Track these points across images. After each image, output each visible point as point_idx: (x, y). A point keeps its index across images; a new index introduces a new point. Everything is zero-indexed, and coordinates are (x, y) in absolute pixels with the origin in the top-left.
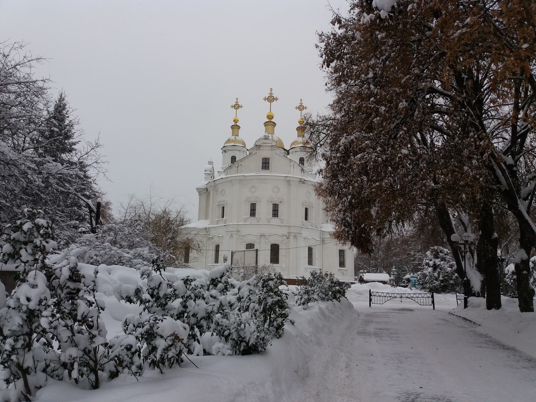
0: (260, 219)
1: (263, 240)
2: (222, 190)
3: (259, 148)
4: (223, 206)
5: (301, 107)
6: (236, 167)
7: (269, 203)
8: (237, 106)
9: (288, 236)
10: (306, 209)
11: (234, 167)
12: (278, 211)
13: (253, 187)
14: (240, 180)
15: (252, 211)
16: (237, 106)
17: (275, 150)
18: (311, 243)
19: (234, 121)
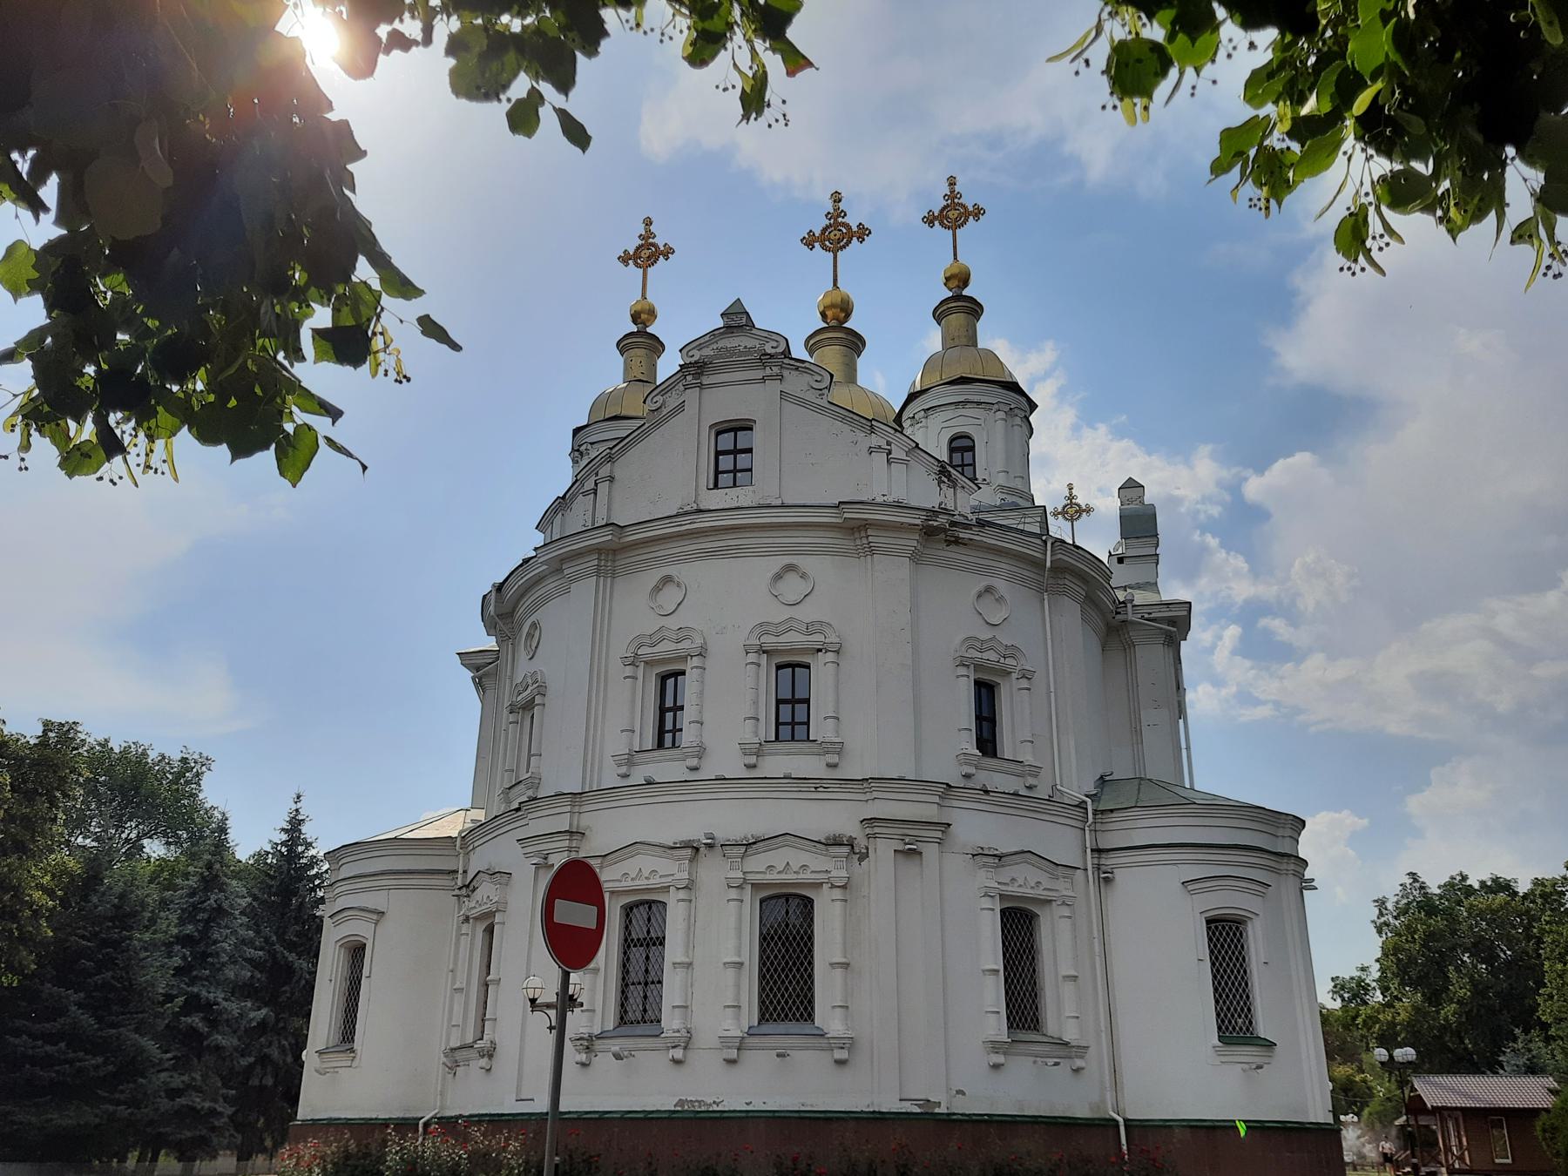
0: (701, 751)
1: (714, 873)
2: (534, 626)
3: (698, 375)
5: (953, 214)
6: (585, 494)
7: (752, 657)
8: (647, 254)
9: (861, 842)
10: (985, 692)
12: (807, 701)
13: (667, 580)
14: (598, 550)
16: (645, 253)
17: (781, 378)
18: (1025, 881)
19: (635, 318)
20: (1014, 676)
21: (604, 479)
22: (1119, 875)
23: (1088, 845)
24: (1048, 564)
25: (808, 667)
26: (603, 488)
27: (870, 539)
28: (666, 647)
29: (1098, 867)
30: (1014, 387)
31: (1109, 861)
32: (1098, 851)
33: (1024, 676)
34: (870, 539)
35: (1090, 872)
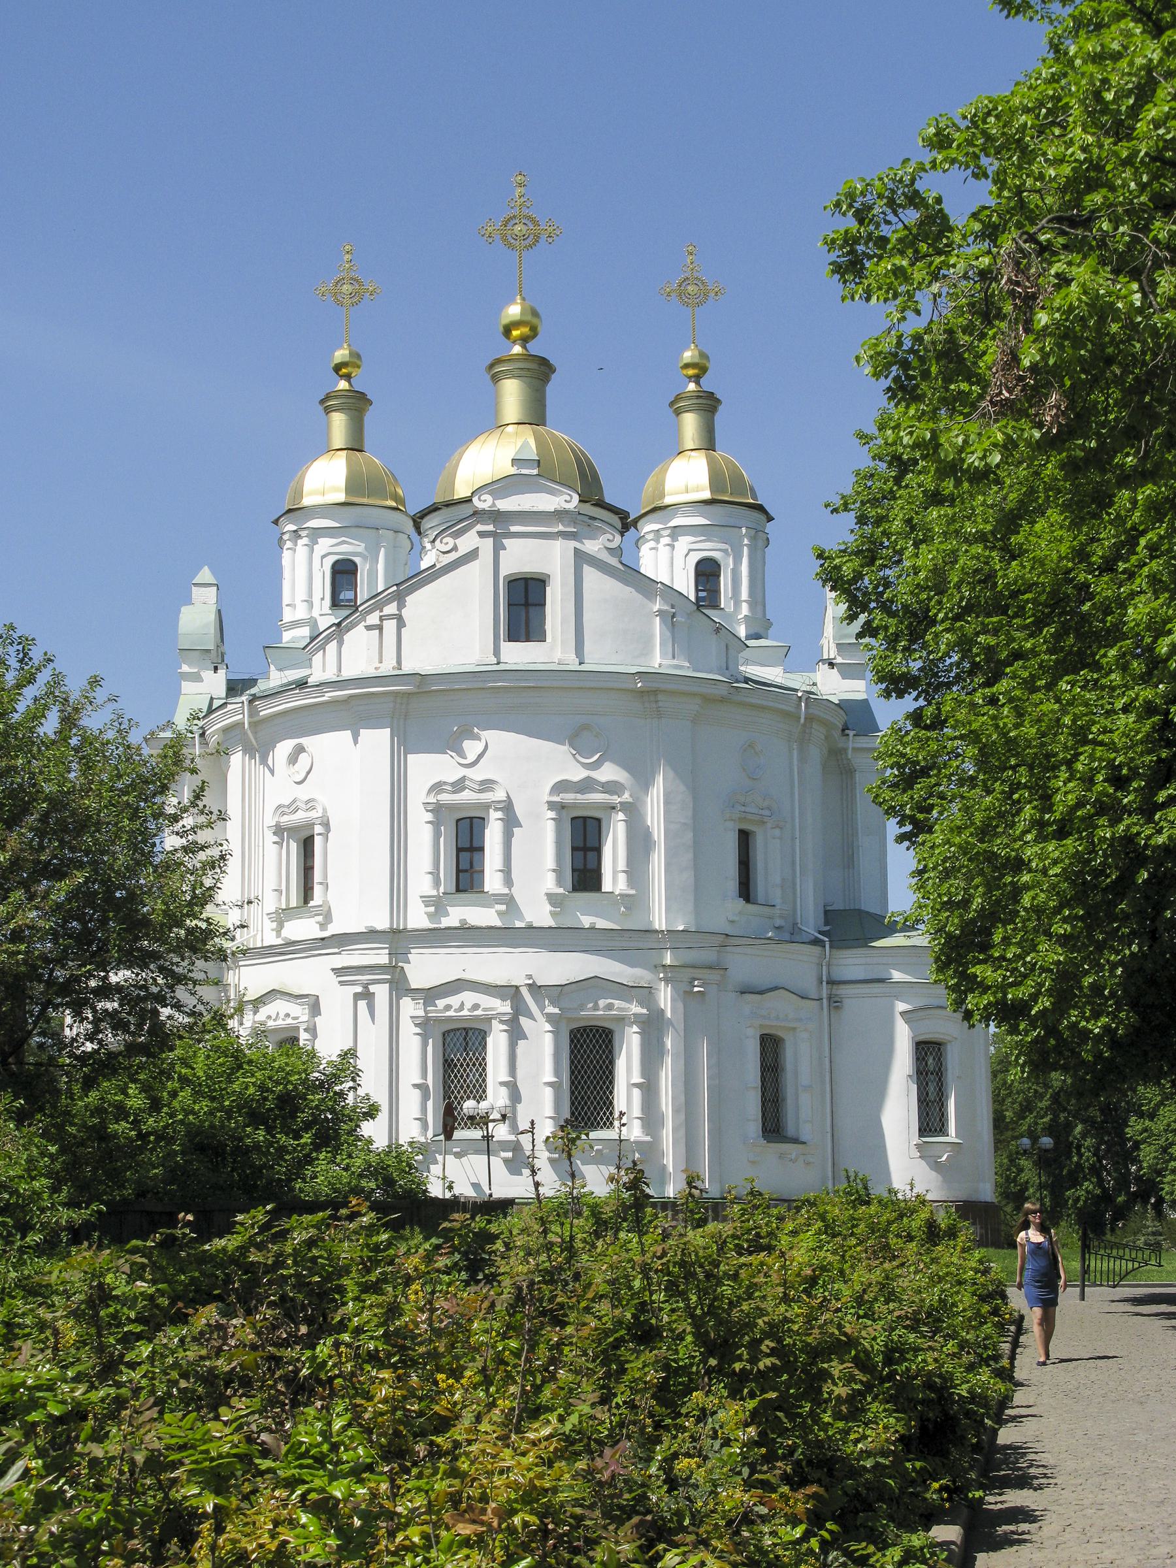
4: (306, 834)
6: (369, 628)
10: (745, 837)
11: (361, 627)
15: (463, 855)
20: (769, 825)
21: (390, 617)
22: (846, 1002)
23: (824, 978)
24: (802, 720)
25: (599, 820)
26: (390, 626)
27: (660, 704)
28: (466, 796)
29: (830, 998)
30: (760, 508)
31: (843, 990)
32: (831, 982)
33: (777, 826)
34: (660, 704)
35: (825, 1001)
